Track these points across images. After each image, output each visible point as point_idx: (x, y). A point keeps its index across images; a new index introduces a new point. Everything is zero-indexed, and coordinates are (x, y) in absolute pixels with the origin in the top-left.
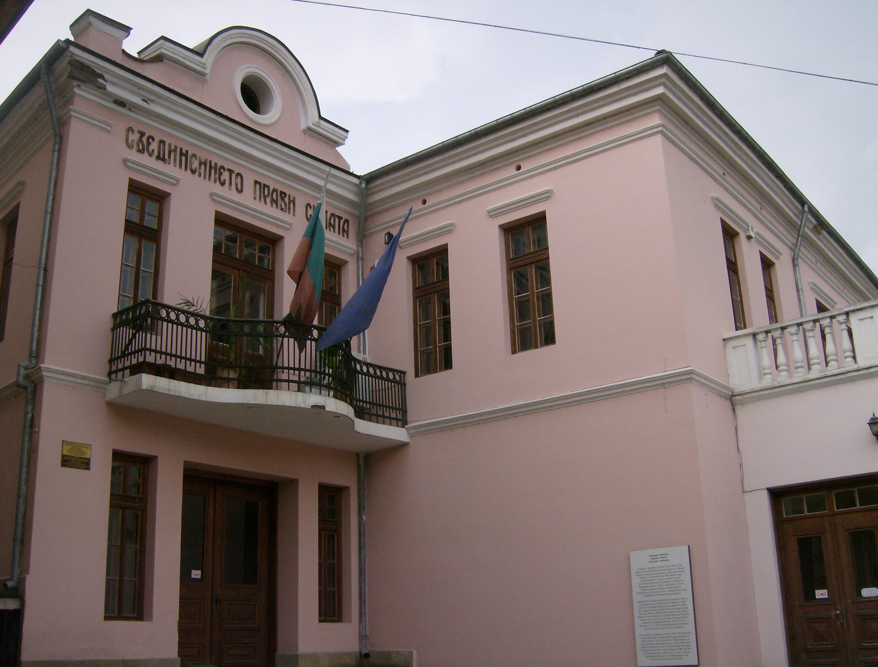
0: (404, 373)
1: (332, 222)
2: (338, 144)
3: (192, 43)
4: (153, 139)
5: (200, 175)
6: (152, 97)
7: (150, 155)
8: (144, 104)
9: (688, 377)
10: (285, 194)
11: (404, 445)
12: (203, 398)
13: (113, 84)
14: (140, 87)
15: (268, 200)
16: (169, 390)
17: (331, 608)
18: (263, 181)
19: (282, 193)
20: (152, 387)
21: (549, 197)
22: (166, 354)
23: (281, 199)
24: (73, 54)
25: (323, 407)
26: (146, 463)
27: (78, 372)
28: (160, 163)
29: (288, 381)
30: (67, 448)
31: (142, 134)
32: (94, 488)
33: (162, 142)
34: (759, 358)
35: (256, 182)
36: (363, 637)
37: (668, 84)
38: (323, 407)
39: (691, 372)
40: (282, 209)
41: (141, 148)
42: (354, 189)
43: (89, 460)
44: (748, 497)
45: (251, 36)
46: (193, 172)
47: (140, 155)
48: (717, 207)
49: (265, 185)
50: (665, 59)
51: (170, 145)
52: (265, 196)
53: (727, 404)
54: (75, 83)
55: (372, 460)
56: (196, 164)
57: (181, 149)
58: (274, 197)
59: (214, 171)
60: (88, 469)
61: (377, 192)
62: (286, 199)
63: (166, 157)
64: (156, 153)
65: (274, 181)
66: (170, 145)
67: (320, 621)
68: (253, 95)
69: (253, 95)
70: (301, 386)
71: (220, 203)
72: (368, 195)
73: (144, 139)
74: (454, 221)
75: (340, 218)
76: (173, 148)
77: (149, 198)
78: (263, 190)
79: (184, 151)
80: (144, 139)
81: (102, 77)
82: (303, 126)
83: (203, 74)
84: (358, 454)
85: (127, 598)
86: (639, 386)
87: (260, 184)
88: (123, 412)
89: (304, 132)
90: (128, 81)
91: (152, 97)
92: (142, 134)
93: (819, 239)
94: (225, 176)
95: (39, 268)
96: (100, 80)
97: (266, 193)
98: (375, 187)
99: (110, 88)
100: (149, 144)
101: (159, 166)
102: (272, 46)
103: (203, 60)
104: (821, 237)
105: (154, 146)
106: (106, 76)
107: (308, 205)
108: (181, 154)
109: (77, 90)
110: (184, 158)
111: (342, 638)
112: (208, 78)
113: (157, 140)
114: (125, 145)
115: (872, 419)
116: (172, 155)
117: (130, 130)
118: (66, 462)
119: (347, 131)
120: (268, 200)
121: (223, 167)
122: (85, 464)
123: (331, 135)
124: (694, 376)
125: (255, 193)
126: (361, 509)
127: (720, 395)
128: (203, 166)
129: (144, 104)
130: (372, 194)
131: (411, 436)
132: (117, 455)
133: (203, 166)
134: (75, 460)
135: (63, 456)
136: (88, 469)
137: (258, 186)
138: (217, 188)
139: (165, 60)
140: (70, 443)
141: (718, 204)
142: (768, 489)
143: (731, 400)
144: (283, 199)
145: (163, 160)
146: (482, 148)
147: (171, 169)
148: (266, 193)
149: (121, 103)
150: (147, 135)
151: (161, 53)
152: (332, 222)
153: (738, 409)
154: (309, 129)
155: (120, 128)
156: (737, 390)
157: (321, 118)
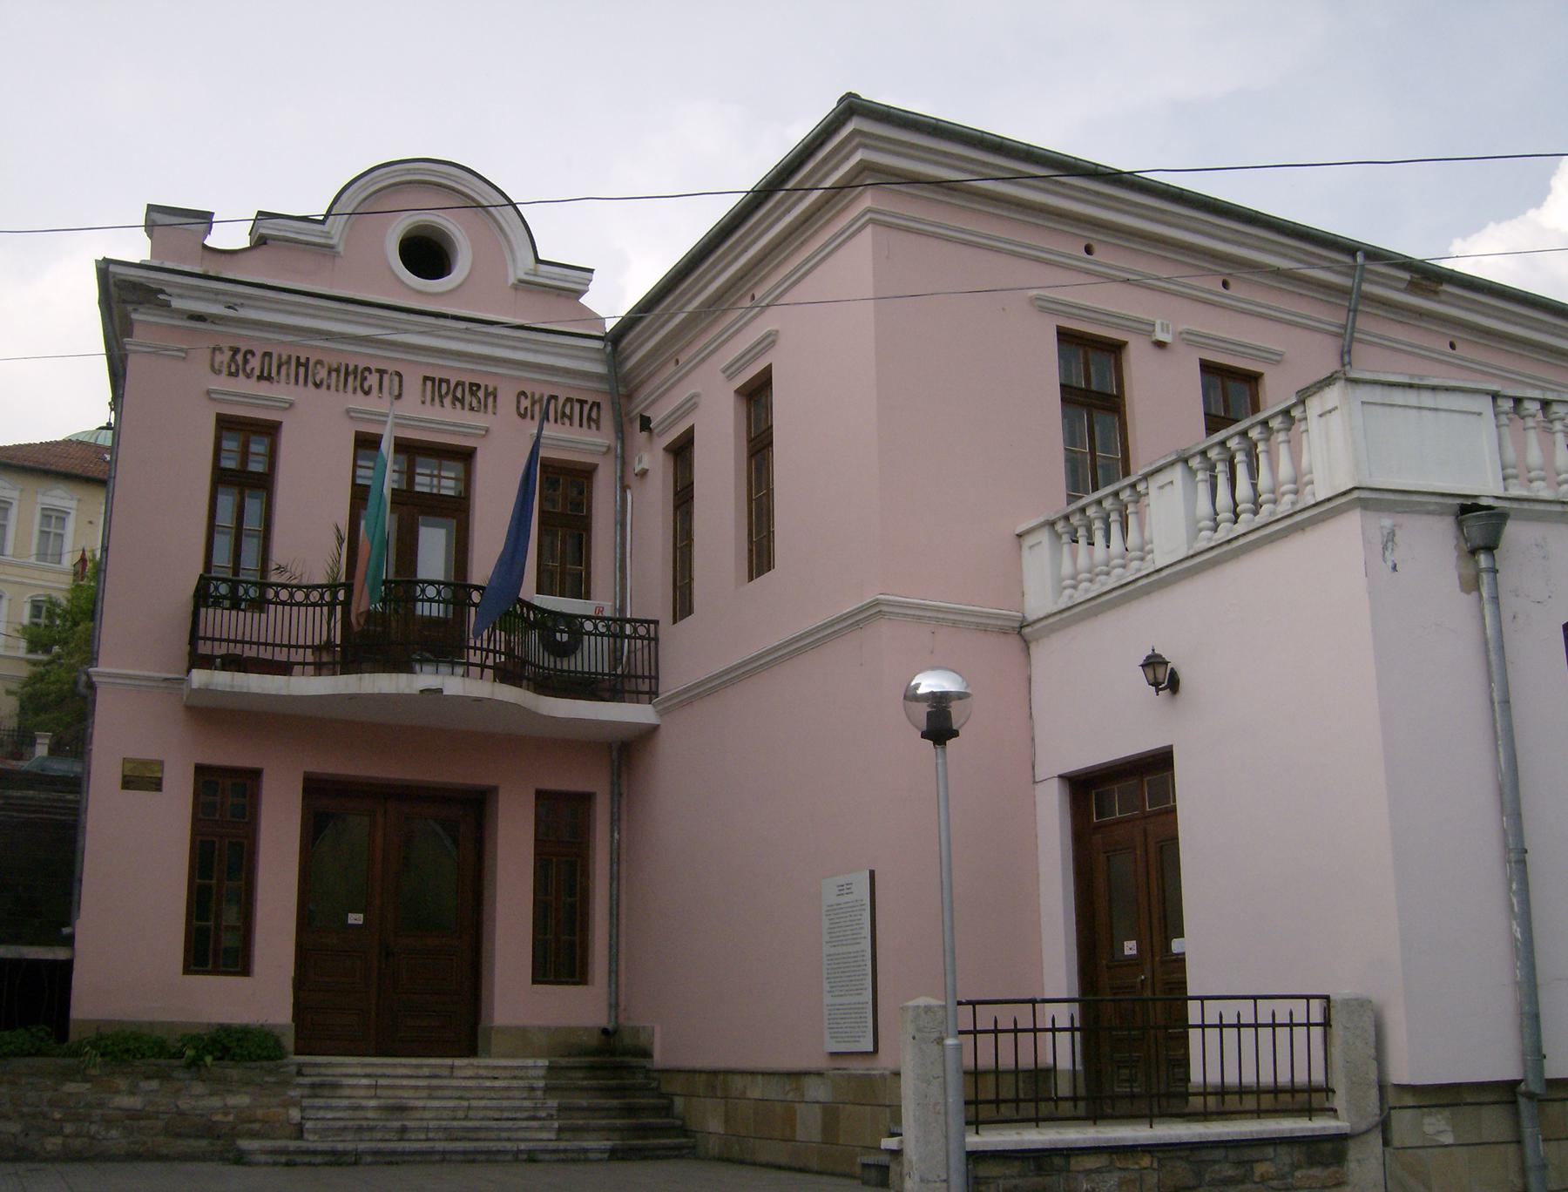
0: (656, 622)
1: (568, 411)
2: (581, 293)
3: (318, 209)
4: (253, 354)
5: (329, 387)
6: (239, 301)
7: (248, 376)
8: (231, 313)
9: (871, 613)
10: (479, 386)
11: (654, 729)
12: (284, 692)
13: (180, 296)
14: (217, 292)
15: (447, 401)
18: (437, 375)
19: (471, 385)
21: (773, 343)
22: (229, 641)
23: (472, 394)
24: (115, 274)
25: (440, 691)
26: (249, 779)
28: (265, 384)
31: (236, 351)
33: (268, 354)
34: (1057, 565)
35: (426, 379)
36: (614, 1006)
37: (867, 141)
38: (440, 691)
39: (877, 603)
40: (472, 409)
42: (597, 356)
44: (1039, 787)
45: (416, 171)
46: (317, 386)
47: (233, 380)
48: (1043, 309)
49: (441, 381)
50: (851, 107)
51: (280, 357)
53: (1014, 643)
54: (130, 308)
55: (626, 753)
56: (322, 373)
58: (459, 395)
59: (354, 377)
60: (160, 790)
61: (633, 352)
62: (481, 394)
63: (274, 374)
64: (257, 372)
65: (455, 372)
66: (280, 357)
67: (534, 982)
68: (426, 254)
69: (426, 254)
71: (362, 419)
72: (622, 363)
73: (239, 358)
74: (699, 390)
75: (582, 402)
76: (284, 358)
77: (255, 433)
78: (437, 388)
79: (303, 360)
80: (239, 358)
81: (163, 292)
82: (512, 280)
83: (332, 247)
84: (610, 745)
86: (836, 628)
87: (433, 380)
89: (515, 287)
90: (198, 288)
91: (239, 301)
92: (236, 351)
93: (1441, 302)
94: (373, 380)
96: (161, 297)
97: (444, 391)
99: (177, 303)
100: (246, 361)
101: (263, 389)
102: (448, 176)
104: (1443, 297)
105: (255, 363)
106: (167, 290)
107: (524, 393)
108: (299, 364)
109: (135, 316)
110: (302, 370)
111: (578, 1008)
112: (341, 248)
113: (259, 355)
114: (208, 368)
115: (1148, 657)
118: (128, 783)
119: (591, 271)
120: (447, 401)
121: (368, 369)
122: (156, 785)
123: (566, 284)
124: (885, 608)
125: (424, 391)
126: (615, 822)
127: (1004, 631)
128: (334, 374)
129: (231, 313)
130: (627, 358)
131: (661, 714)
133: (334, 374)
134: (142, 778)
136: (160, 790)
137: (429, 384)
138: (359, 402)
141: (1045, 307)
142: (1060, 777)
143: (1019, 633)
144: (473, 394)
145: (269, 378)
146: (709, 276)
147: (281, 391)
148: (444, 391)
149: (200, 318)
150: (243, 350)
151: (270, 233)
152: (568, 411)
153: (1033, 647)
154: (521, 281)
156: (1031, 617)
157: (538, 261)
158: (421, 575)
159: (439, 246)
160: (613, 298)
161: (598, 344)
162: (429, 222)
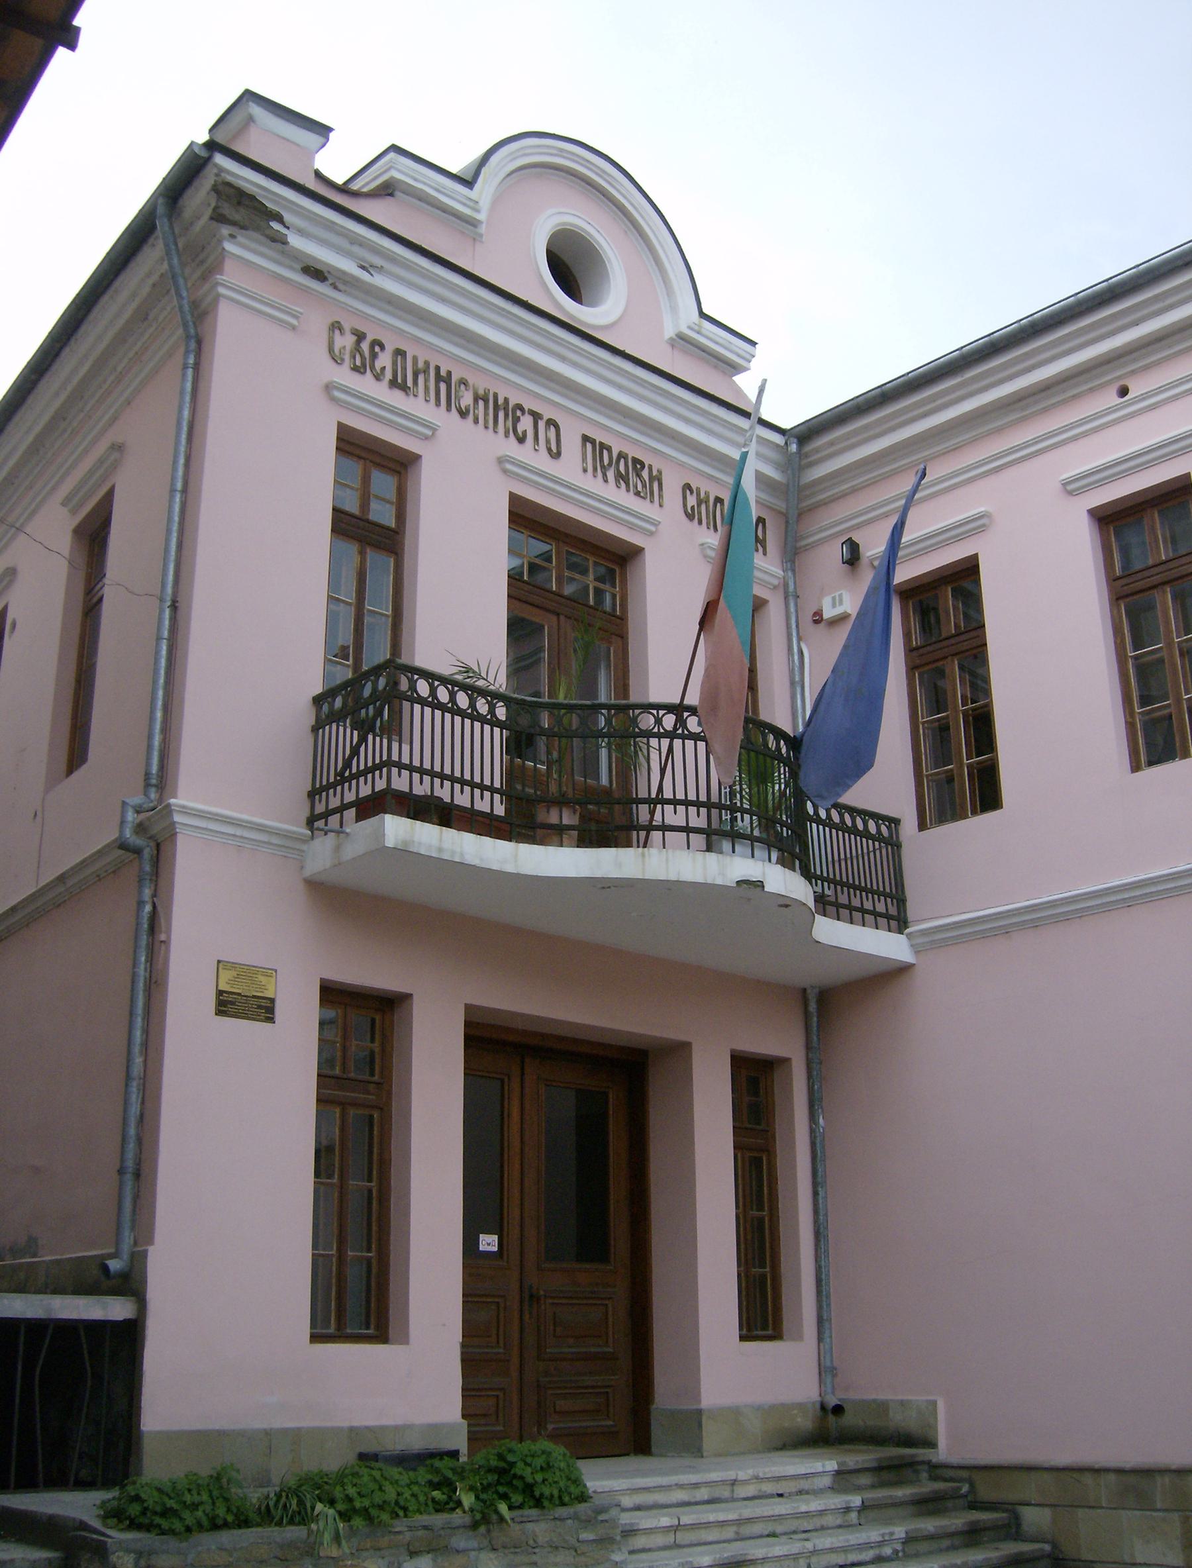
0: (894, 822)
2: (736, 369)
4: (382, 347)
5: (476, 421)
7: (378, 378)
8: (364, 276)
11: (903, 970)
12: (510, 868)
13: (301, 232)
15: (611, 474)
16: (440, 850)
17: (761, 1316)
18: (599, 437)
19: (636, 461)
20: (405, 842)
22: (432, 774)
23: (634, 473)
24: (221, 170)
25: (760, 885)
27: (245, 817)
28: (398, 394)
29: (687, 830)
30: (225, 976)
31: (360, 337)
32: (284, 1064)
33: (400, 353)
35: (586, 439)
36: (826, 1371)
38: (760, 885)
40: (637, 494)
41: (358, 363)
43: (272, 1000)
46: (463, 414)
47: (356, 376)
51: (415, 359)
52: (603, 467)
54: (225, 230)
55: (835, 1004)
56: (467, 400)
57: (438, 368)
59: (503, 413)
60: (271, 1020)
62: (645, 474)
63: (410, 383)
64: (388, 375)
66: (415, 359)
67: (742, 1338)
68: (570, 267)
69: (570, 267)
70: (714, 838)
72: (802, 468)
73: (365, 346)
74: (990, 509)
76: (421, 365)
77: (381, 466)
78: (598, 453)
79: (443, 373)
80: (365, 346)
81: (279, 219)
82: (669, 332)
83: (473, 223)
85: (355, 1297)
87: (593, 442)
88: (340, 902)
89: (672, 343)
90: (330, 226)
91: (378, 261)
92: (360, 337)
94: (526, 423)
95: (162, 600)
96: (275, 225)
97: (606, 462)
98: (817, 450)
99: (295, 241)
100: (374, 356)
101: (396, 399)
102: (602, 173)
103: (473, 194)
105: (384, 360)
106: (287, 217)
107: (687, 487)
108: (439, 378)
109: (229, 246)
110: (443, 386)
112: (483, 229)
113: (389, 348)
116: (421, 379)
117: (336, 327)
118: (226, 1005)
119: (754, 344)
121: (519, 407)
122: (265, 1010)
123: (719, 351)
125: (584, 459)
128: (481, 403)
129: (364, 276)
130: (811, 465)
132: (330, 993)
133: (481, 403)
134: (242, 1004)
135: (220, 993)
137: (589, 446)
138: (510, 447)
139: (397, 193)
140: (233, 965)
144: (639, 476)
145: (404, 388)
147: (418, 407)
148: (606, 462)
149: (316, 272)
151: (392, 180)
154: (681, 337)
155: (316, 322)
157: (703, 315)
159: (568, 268)
160: (793, 385)
161: (778, 439)
162: (588, 229)
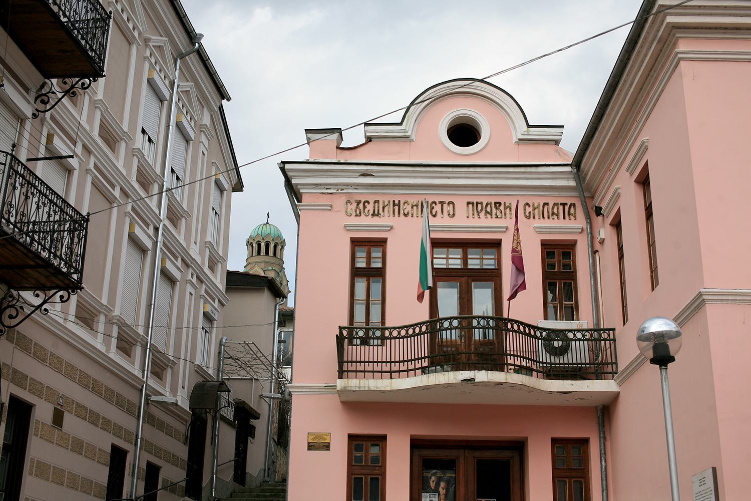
0: (614, 330)
1: (555, 211)
4: (368, 202)
10: (500, 204)
15: (482, 214)
16: (359, 387)
18: (474, 200)
19: (496, 203)
20: (345, 387)
25: (474, 380)
27: (317, 385)
30: (311, 437)
31: (359, 203)
32: (336, 463)
35: (468, 203)
40: (497, 217)
41: (358, 212)
43: (329, 443)
49: (477, 203)
51: (384, 202)
52: (478, 212)
56: (409, 208)
57: (394, 201)
60: (329, 450)
63: (381, 212)
66: (384, 202)
68: (464, 133)
69: (464, 133)
72: (584, 179)
73: (361, 206)
74: (620, 186)
75: (564, 205)
77: (372, 246)
79: (397, 202)
80: (361, 206)
82: (515, 140)
87: (473, 203)
88: (355, 405)
94: (438, 208)
100: (365, 207)
101: (376, 221)
103: (403, 126)
105: (370, 207)
107: (527, 204)
108: (394, 205)
110: (396, 208)
112: (413, 137)
116: (386, 209)
117: (348, 202)
118: (311, 447)
119: (562, 127)
120: (482, 214)
122: (327, 447)
125: (468, 210)
126: (603, 454)
128: (415, 208)
130: (586, 174)
131: (620, 384)
132: (351, 437)
134: (318, 445)
135: (309, 443)
136: (329, 450)
137: (470, 206)
139: (372, 140)
140: (314, 434)
147: (385, 220)
152: (555, 211)
154: (520, 140)
155: (339, 202)
157: (529, 126)
158: (475, 313)
159: (472, 126)
161: (568, 169)
